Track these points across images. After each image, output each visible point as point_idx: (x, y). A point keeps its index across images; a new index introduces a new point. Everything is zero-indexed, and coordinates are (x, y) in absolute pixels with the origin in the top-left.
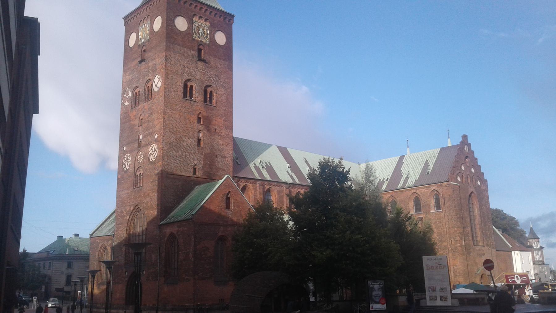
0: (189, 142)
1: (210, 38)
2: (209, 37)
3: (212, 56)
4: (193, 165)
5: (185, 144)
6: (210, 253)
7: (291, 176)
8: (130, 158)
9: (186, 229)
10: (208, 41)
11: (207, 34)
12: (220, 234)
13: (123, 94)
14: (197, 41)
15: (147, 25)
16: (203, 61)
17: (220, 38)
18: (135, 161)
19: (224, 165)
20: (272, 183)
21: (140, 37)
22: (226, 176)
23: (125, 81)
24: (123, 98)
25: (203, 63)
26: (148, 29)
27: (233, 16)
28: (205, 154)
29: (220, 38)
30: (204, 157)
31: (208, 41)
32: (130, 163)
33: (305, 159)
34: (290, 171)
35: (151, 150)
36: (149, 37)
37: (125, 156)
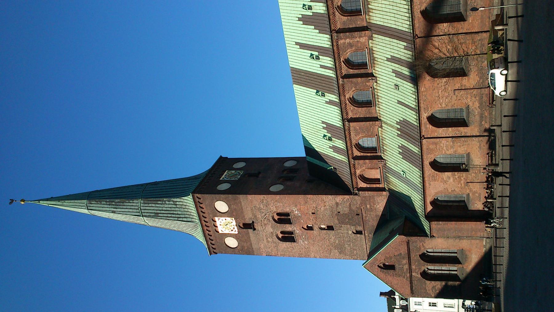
3: (244, 216)
4: (353, 235)
5: (337, 242)
6: (437, 285)
12: (420, 276)
19: (345, 205)
28: (339, 223)
30: (343, 224)
33: (297, 44)
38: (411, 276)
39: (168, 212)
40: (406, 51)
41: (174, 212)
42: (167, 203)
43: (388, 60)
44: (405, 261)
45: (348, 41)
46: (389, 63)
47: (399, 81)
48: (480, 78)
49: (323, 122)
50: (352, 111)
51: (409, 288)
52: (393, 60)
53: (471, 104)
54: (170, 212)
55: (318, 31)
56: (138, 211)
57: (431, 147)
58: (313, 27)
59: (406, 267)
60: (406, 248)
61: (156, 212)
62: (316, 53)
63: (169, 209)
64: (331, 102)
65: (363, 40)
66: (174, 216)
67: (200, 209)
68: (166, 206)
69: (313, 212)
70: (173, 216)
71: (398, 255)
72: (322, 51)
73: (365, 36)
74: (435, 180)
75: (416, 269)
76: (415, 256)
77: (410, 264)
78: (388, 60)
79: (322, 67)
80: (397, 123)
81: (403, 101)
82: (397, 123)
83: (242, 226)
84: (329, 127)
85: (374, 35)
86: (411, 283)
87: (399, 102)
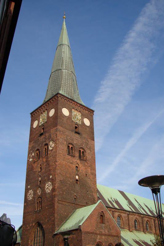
1: (81, 121)
2: (81, 121)
7: (130, 208)
8: (33, 192)
9: (75, 236)
10: (80, 123)
11: (80, 119)
12: (98, 240)
13: (29, 155)
14: (75, 122)
15: (45, 114)
16: (79, 133)
17: (87, 122)
18: (35, 194)
20: (120, 211)
21: (40, 122)
22: (99, 201)
23: (30, 147)
24: (29, 157)
25: (78, 135)
26: (46, 116)
27: (93, 111)
29: (87, 122)
31: (80, 123)
32: (33, 195)
34: (128, 205)
35: (48, 185)
36: (46, 120)
37: (29, 191)
50: (133, 218)
51: (88, 231)
59: (103, 232)
69: (87, 175)
71: (110, 228)
75: (102, 239)
77: (105, 235)
83: (76, 126)
86: (92, 233)
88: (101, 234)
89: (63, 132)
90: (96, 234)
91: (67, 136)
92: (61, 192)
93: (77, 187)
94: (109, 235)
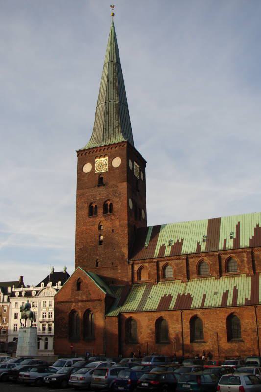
0: (93, 245)
4: (96, 259)
12: (72, 308)
33: (239, 223)
38: (72, 302)
39: (110, 121)
40: (244, 300)
41: (110, 126)
42: (117, 122)
43: (235, 287)
44: (84, 298)
45: (246, 259)
46: (233, 288)
47: (221, 295)
48: (226, 351)
49: (182, 240)
50: (194, 261)
51: (62, 300)
52: (236, 292)
53: (208, 344)
54: (110, 123)
55: (251, 238)
56: (110, 99)
57: (175, 317)
58: (253, 235)
59: (80, 299)
60: (95, 299)
61: (110, 112)
62: (234, 236)
63: (112, 123)
64: (199, 246)
65: (246, 270)
66: (107, 126)
67: (114, 146)
68: (114, 120)
70: (107, 125)
71: (89, 293)
72: (237, 241)
73: (249, 271)
74: (149, 320)
75: (78, 305)
76: (89, 305)
77: (82, 301)
78: (235, 287)
79: (225, 241)
80: (188, 294)
81: (206, 297)
82: (188, 294)
83: (101, 176)
84: (179, 245)
85: (250, 278)
86: (66, 302)
87: (205, 295)
88: (77, 302)
89: (83, 194)
90: (72, 302)
91: (89, 196)
92: (81, 261)
93: (101, 248)
94: (87, 301)
